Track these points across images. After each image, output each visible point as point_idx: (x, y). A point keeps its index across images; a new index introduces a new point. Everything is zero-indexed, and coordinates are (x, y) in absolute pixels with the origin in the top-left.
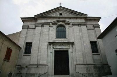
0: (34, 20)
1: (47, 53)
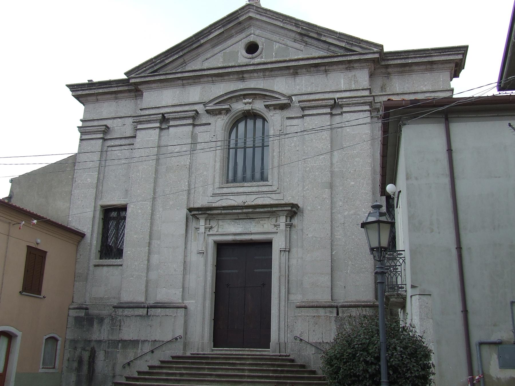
0: (130, 91)
1: (185, 256)
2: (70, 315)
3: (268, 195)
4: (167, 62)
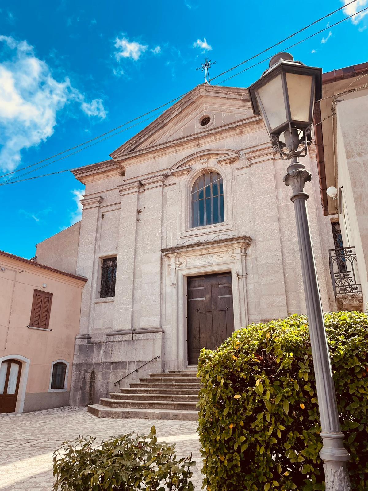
1: (161, 289)
2: (76, 344)
3: (225, 233)
4: (140, 141)
